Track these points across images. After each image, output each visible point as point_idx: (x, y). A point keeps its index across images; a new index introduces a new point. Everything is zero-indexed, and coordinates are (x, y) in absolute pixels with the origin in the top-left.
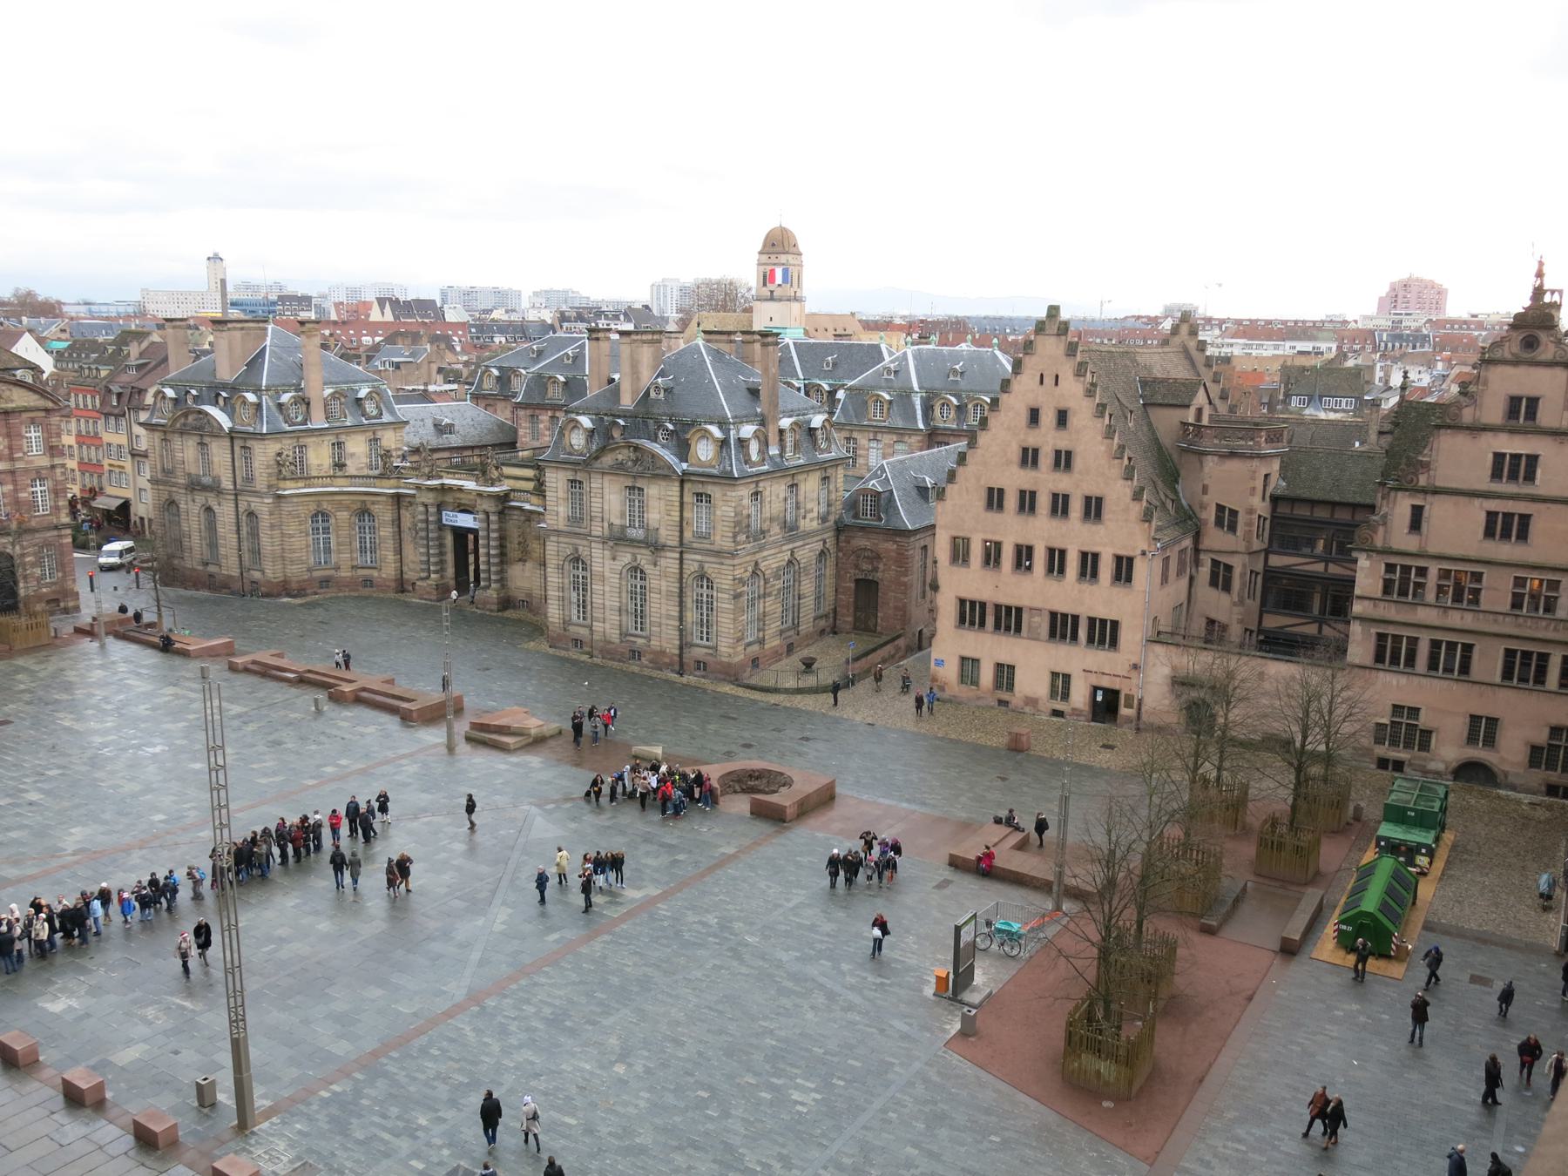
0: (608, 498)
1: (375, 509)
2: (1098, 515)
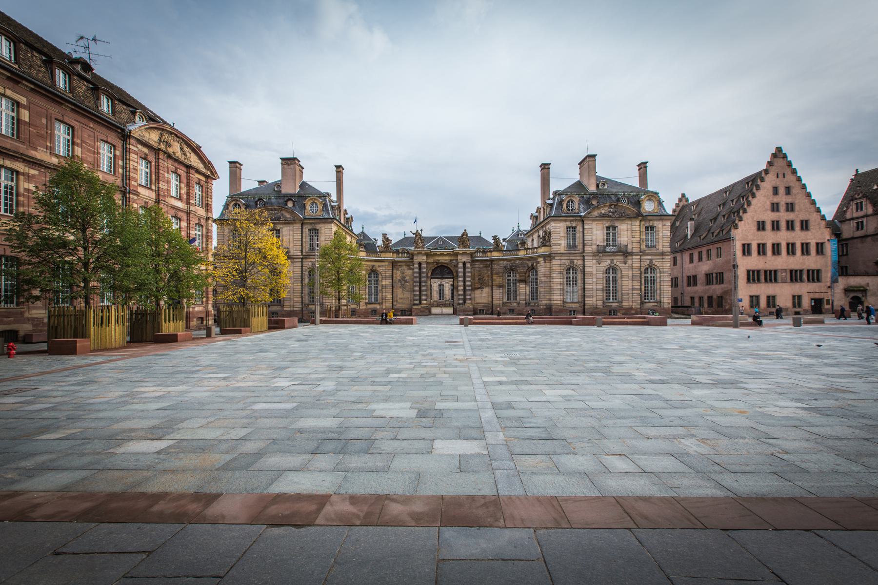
0: (596, 233)
1: (380, 269)
2: (807, 229)
